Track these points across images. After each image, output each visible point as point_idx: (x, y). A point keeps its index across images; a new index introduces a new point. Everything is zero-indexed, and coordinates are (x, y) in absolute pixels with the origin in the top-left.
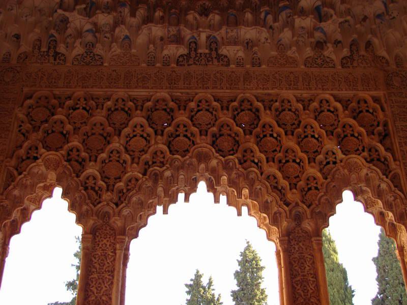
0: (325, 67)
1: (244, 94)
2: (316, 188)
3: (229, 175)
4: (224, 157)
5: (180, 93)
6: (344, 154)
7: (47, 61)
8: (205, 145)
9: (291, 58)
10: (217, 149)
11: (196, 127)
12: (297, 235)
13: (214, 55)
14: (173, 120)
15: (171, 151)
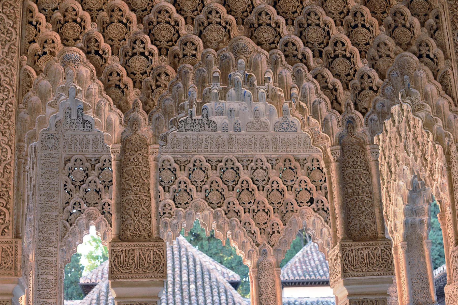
0: (289, 131)
1: (228, 155)
2: (279, 232)
3: (218, 222)
4: (214, 209)
5: (182, 155)
6: (299, 206)
7: (77, 128)
8: (201, 199)
9: (264, 122)
10: (209, 201)
11: (193, 184)
12: (264, 265)
13: (205, 122)
14: (176, 178)
15: (176, 204)
